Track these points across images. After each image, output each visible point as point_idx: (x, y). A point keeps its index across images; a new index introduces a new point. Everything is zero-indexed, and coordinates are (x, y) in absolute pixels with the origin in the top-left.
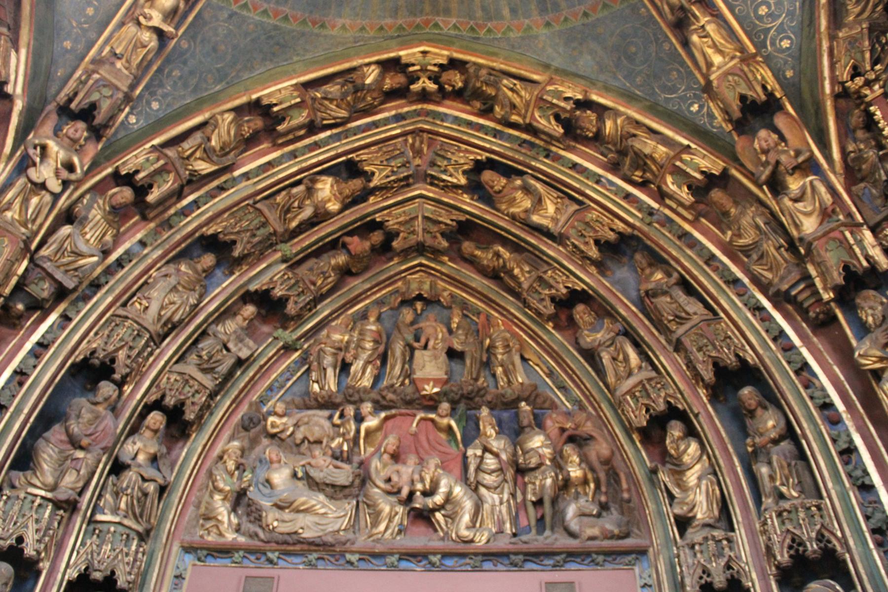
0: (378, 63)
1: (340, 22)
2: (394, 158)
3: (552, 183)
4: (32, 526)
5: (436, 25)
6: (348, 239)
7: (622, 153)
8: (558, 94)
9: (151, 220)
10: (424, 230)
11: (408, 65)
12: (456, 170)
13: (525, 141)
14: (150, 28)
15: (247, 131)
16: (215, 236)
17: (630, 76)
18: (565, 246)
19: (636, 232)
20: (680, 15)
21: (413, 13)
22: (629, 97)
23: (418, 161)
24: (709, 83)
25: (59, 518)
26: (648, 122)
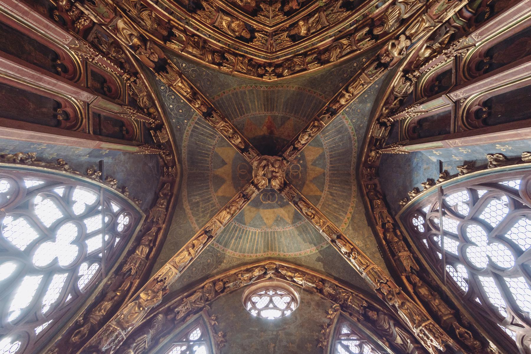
0: (284, 76)
1: (294, 89)
2: (279, 43)
3: (225, 34)
5: (267, 87)
6: (298, 8)
7: (204, 48)
8: (228, 68)
9: (370, 18)
10: (269, 12)
11: (275, 75)
12: (259, 39)
13: (237, 50)
14: (350, 93)
15: (327, 55)
16: (347, 11)
17: (207, 74)
18: (216, 6)
19: (190, 14)
20: (195, 97)
21: (273, 91)
22: (206, 67)
23: (272, 42)
24: (180, 77)
26: (198, 60)
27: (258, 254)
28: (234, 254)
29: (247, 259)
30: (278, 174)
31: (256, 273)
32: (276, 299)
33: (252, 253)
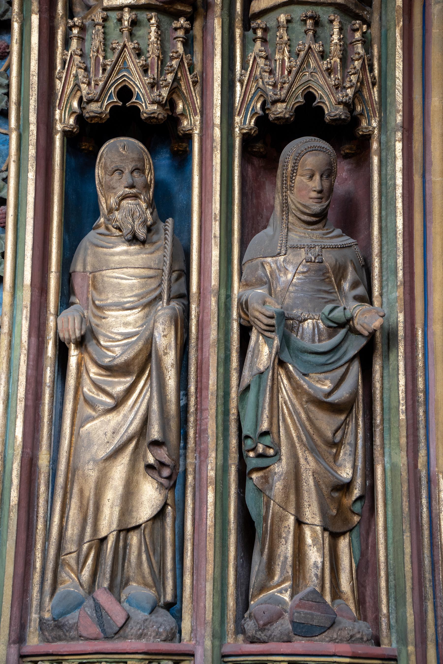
4: (133, 64)
25: (181, 33)
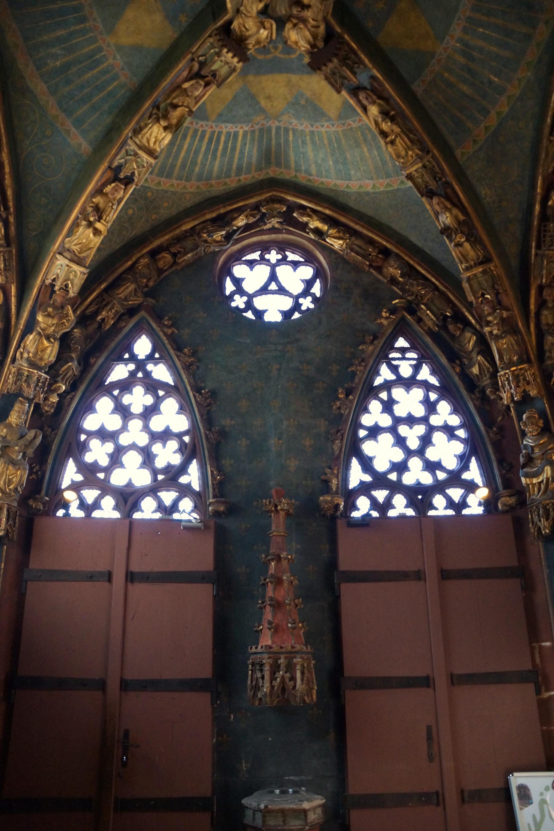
27: (242, 177)
28: (185, 187)
29: (218, 189)
30: (308, 14)
31: (241, 222)
32: (283, 272)
33: (229, 176)
